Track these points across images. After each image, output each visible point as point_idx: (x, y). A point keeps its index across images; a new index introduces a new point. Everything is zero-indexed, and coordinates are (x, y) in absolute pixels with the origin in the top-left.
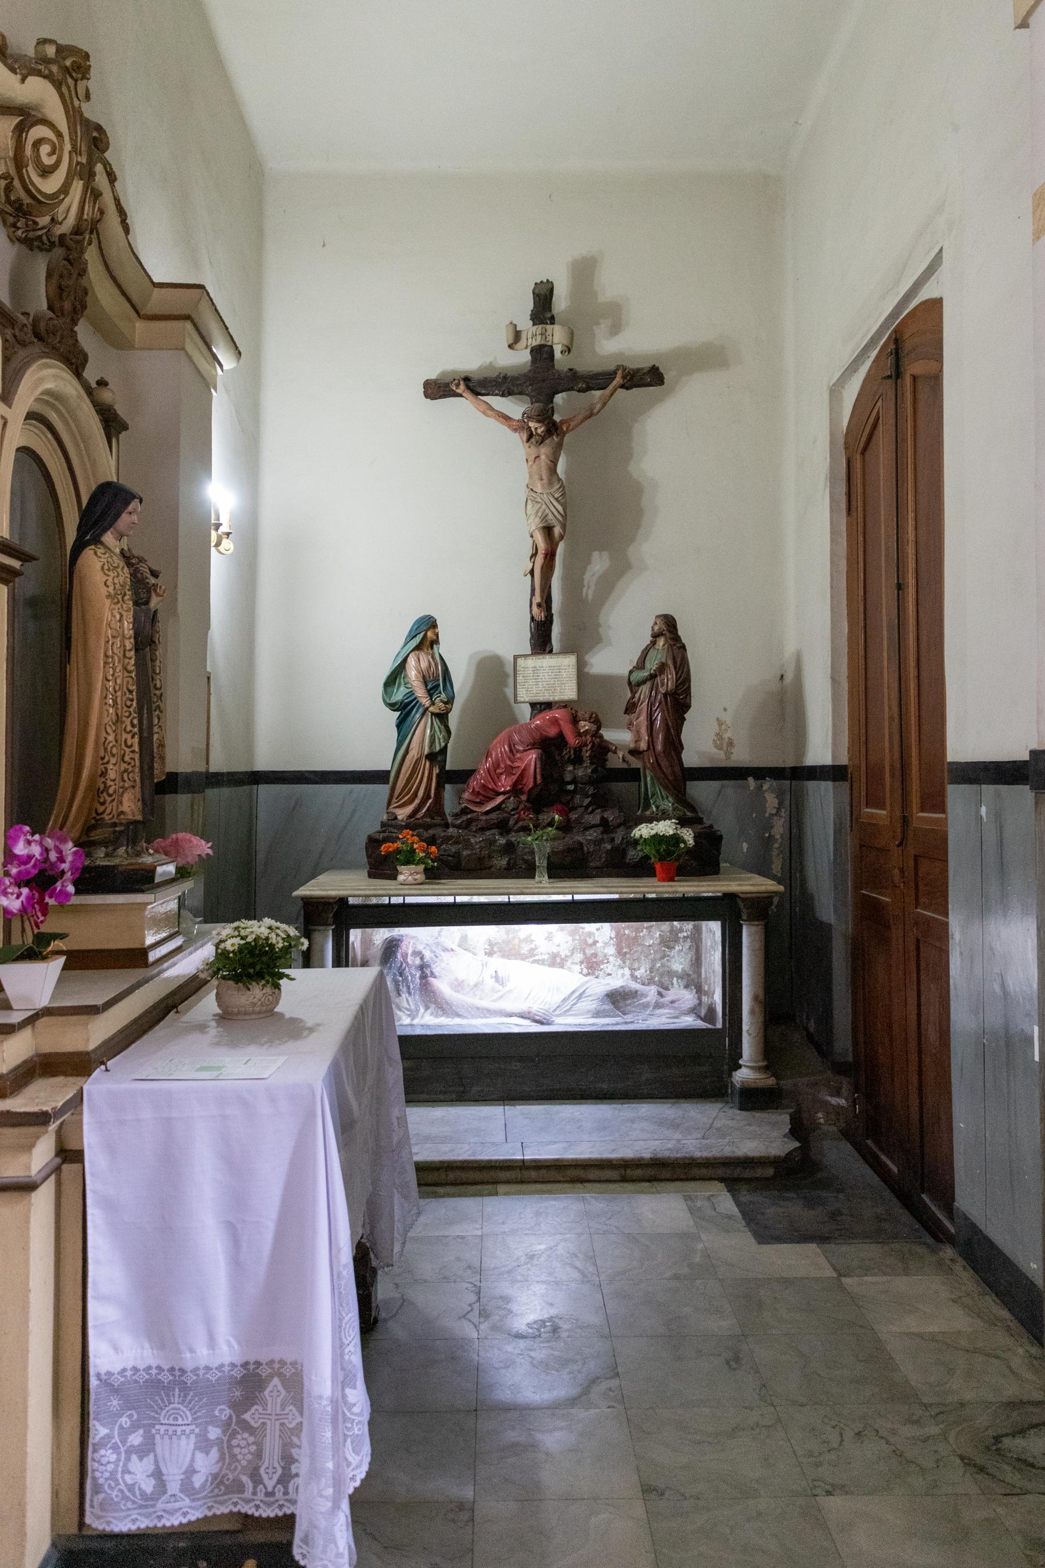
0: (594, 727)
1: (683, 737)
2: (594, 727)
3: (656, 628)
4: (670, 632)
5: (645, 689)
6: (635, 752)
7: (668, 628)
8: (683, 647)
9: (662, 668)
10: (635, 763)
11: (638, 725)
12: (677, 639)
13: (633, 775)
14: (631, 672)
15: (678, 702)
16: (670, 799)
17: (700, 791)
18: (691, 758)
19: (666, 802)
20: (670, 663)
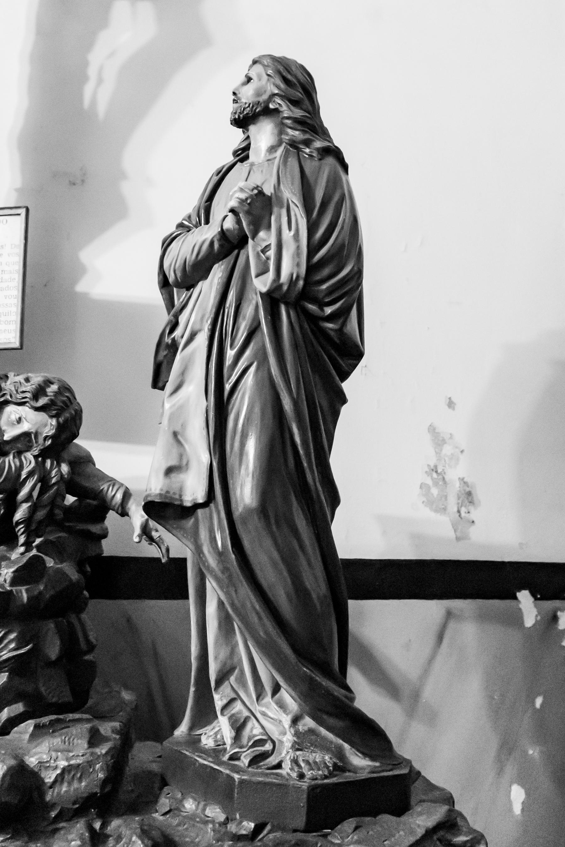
0: (47, 425)
1: (337, 461)
2: (47, 425)
3: (248, 94)
4: (295, 103)
5: (208, 289)
6: (165, 510)
7: (290, 99)
8: (334, 153)
9: (259, 208)
10: (173, 544)
11: (178, 413)
12: (312, 125)
13: (168, 580)
14: (168, 242)
15: (317, 332)
16: (286, 695)
17: (386, 626)
18: (361, 531)
19: (269, 708)
20: (291, 194)
